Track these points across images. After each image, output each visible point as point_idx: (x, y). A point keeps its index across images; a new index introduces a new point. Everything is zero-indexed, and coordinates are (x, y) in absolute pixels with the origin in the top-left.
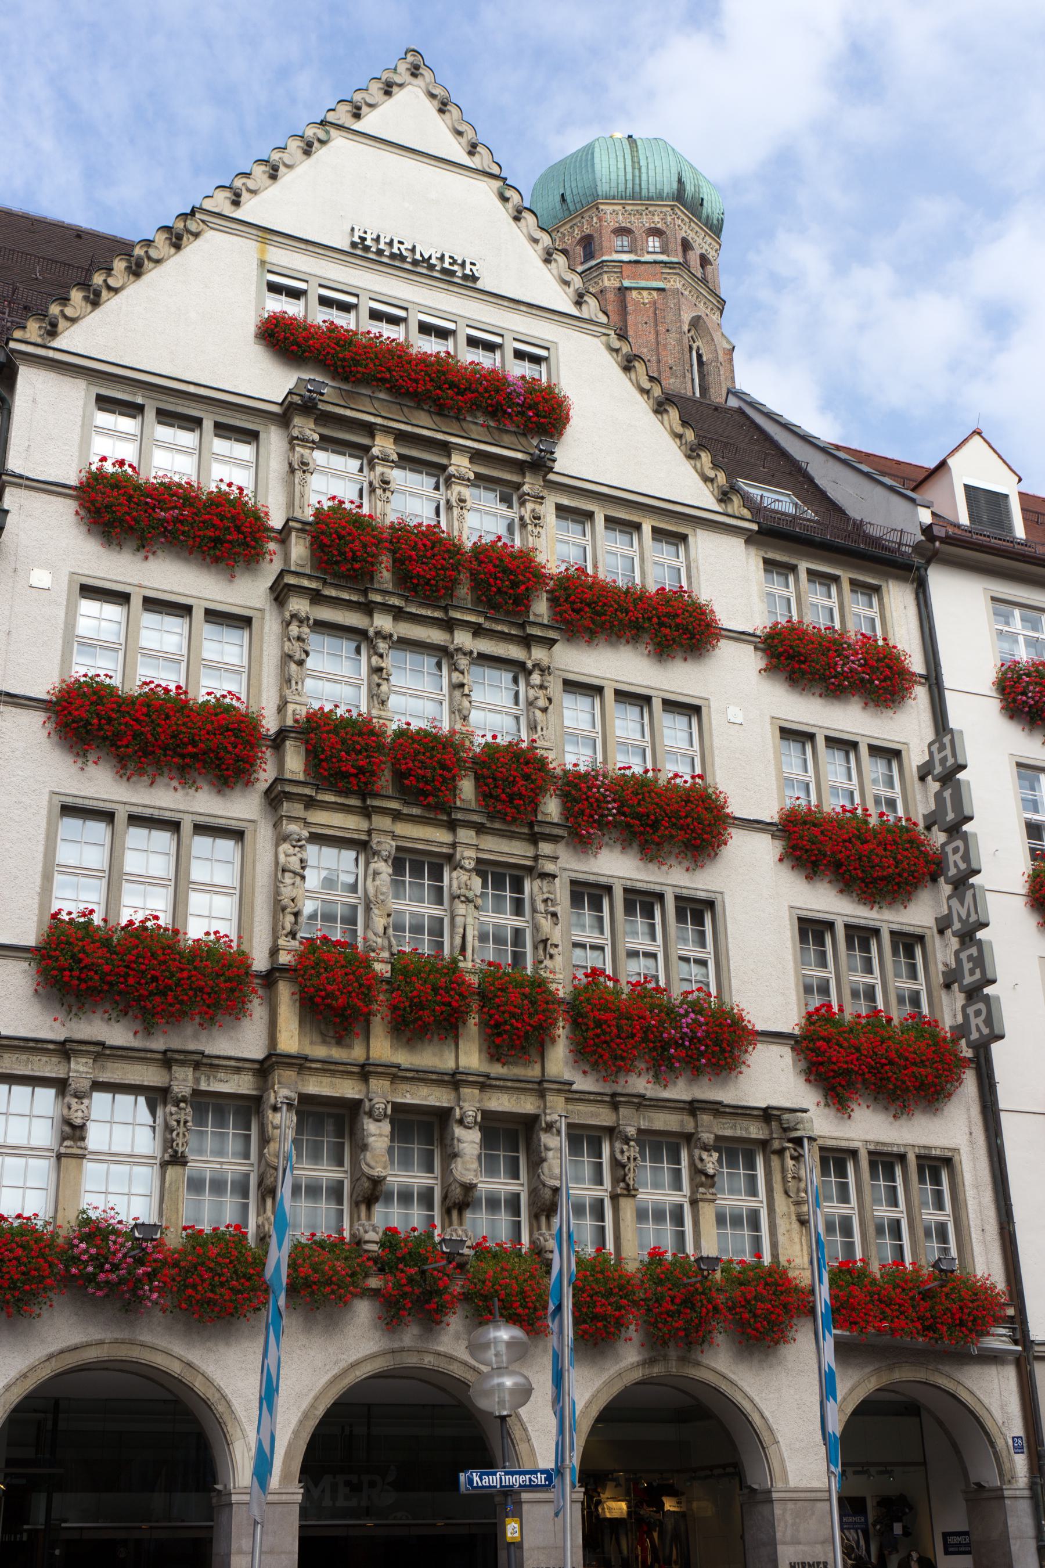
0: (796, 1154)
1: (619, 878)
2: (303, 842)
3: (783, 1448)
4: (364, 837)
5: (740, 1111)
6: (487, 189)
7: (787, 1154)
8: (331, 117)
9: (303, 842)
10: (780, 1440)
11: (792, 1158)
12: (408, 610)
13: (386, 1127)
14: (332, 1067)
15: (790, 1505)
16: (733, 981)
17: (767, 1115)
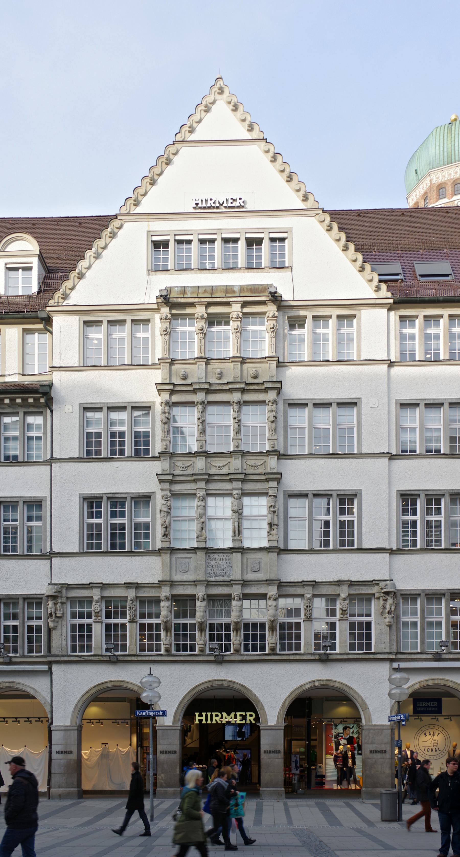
0: (385, 598)
1: (311, 491)
2: (169, 499)
3: (371, 711)
4: (195, 492)
5: (360, 583)
6: (256, 150)
7: (381, 599)
8: (179, 138)
9: (169, 499)
10: (370, 708)
11: (384, 600)
12: (212, 388)
13: (204, 603)
14: (183, 583)
15: (372, 731)
16: (363, 528)
17: (373, 583)
